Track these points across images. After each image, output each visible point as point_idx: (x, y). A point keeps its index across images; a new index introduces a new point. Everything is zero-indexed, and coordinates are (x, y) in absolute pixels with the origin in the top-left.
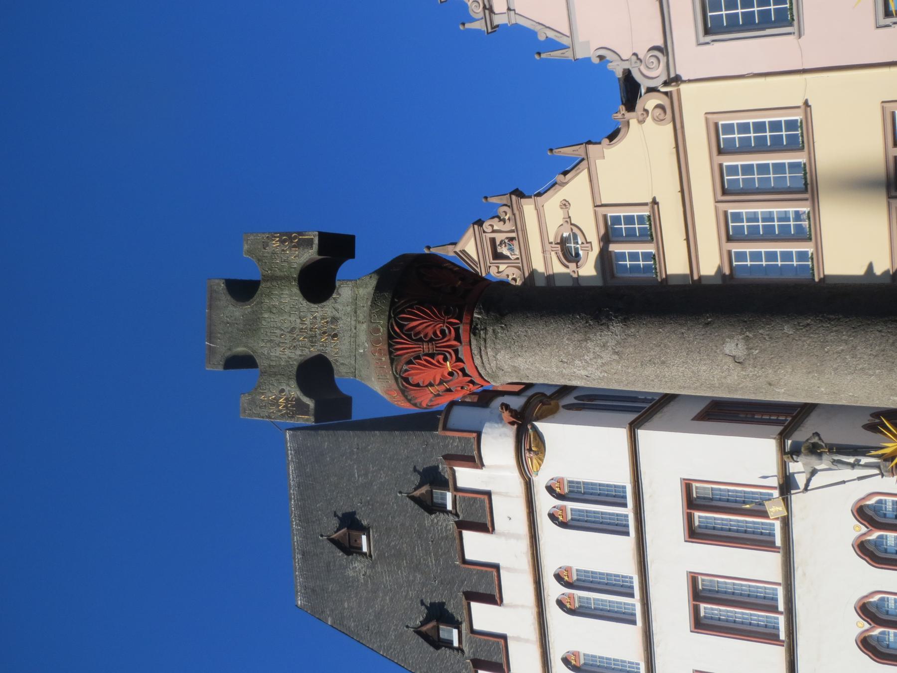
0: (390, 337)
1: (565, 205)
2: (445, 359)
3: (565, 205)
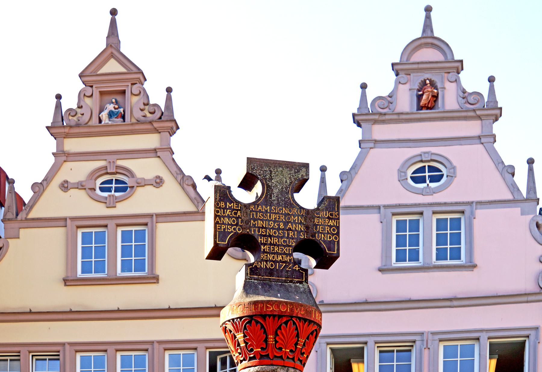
0: (280, 316)
1: (158, 182)
2: (262, 348)
3: (158, 182)
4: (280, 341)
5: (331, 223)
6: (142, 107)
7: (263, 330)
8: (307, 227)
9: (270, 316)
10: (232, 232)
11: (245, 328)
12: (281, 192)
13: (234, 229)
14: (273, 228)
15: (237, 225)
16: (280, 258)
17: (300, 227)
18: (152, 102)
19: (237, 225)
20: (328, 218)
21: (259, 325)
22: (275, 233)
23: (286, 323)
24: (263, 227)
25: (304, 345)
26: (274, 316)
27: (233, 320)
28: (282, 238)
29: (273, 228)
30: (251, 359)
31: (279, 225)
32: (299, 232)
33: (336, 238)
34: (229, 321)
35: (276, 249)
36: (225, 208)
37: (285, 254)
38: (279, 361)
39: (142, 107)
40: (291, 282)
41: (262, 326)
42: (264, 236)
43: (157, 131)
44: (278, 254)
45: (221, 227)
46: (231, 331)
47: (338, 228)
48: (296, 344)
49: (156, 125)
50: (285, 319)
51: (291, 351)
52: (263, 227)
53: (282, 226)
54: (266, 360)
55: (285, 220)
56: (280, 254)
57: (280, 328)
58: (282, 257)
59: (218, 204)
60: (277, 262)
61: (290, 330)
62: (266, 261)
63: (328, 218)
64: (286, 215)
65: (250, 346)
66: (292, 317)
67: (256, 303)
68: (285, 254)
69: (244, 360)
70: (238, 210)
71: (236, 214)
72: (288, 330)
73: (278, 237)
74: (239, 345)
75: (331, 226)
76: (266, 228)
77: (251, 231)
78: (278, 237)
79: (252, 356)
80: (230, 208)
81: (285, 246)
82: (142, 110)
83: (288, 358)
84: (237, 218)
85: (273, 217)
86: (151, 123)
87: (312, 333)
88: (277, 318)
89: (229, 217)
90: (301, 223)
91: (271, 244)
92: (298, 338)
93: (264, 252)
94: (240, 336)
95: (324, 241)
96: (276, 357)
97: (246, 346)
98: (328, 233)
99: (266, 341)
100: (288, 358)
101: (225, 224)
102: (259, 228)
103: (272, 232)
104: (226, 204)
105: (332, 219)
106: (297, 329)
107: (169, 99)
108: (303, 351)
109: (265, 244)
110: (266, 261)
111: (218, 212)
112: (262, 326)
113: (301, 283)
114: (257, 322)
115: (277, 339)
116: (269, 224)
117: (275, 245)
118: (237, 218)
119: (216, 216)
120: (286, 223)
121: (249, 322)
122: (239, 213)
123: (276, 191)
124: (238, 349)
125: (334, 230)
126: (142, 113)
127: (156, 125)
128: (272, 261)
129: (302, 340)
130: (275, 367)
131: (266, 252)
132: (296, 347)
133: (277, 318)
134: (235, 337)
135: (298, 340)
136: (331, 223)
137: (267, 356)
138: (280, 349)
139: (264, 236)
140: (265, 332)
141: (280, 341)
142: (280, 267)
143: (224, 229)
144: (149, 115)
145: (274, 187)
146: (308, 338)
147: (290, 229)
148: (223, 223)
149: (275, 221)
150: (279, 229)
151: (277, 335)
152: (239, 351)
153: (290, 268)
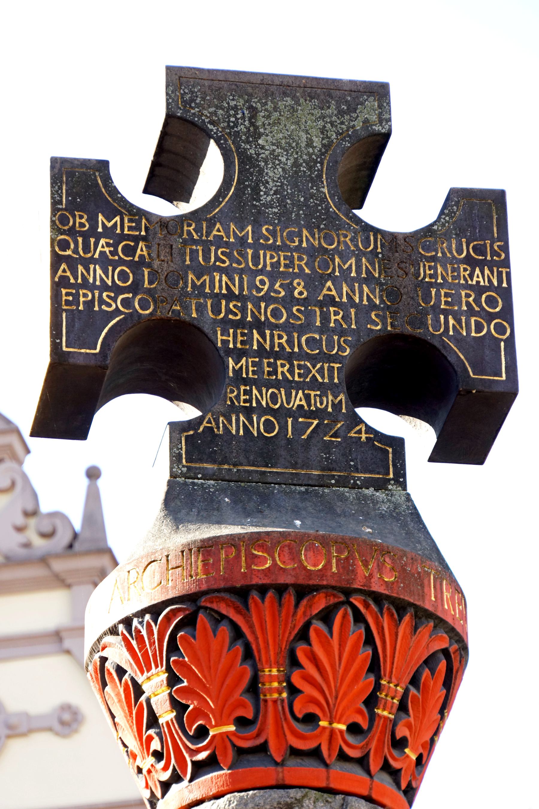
0: (303, 591)
1: (67, 721)
2: (241, 722)
3: (67, 721)
4: (308, 689)
5: (479, 278)
6: (20, 520)
7: (239, 647)
8: (393, 294)
9: (263, 590)
10: (117, 312)
11: (173, 648)
12: (294, 176)
13: (126, 303)
14: (267, 299)
15: (135, 288)
16: (298, 399)
17: (365, 294)
18: (45, 508)
19: (135, 288)
20: (468, 260)
21: (224, 628)
22: (276, 314)
23: (327, 617)
24: (230, 296)
25: (403, 707)
26: (281, 589)
27: (127, 622)
28: (302, 330)
29: (267, 299)
30: (200, 768)
31: (290, 288)
32: (364, 311)
33: (500, 329)
34: (113, 631)
35: (283, 369)
36: (93, 232)
37: (314, 384)
38: (309, 771)
39: (20, 520)
40: (342, 482)
41: (238, 633)
42: (236, 325)
43: (61, 582)
44: (289, 386)
45: (76, 296)
46: (121, 671)
47: (507, 294)
48: (371, 701)
49: (58, 566)
50: (321, 603)
51: (354, 729)
52: (230, 296)
53: (300, 290)
54: (261, 770)
55: (312, 269)
56: (299, 386)
57: (303, 635)
58: (307, 397)
59: (64, 220)
60: (289, 413)
61: (342, 645)
62: (248, 412)
63: (468, 260)
64: (313, 253)
65: (198, 713)
66: (348, 592)
67: (207, 548)
68: (314, 384)
69: (176, 778)
70: (137, 239)
71: (130, 251)
72: (337, 649)
73: (287, 328)
74: (153, 721)
75: (479, 290)
76: (240, 297)
77: (186, 308)
78: (287, 328)
79: (202, 756)
80: (108, 232)
81: (314, 359)
82: (20, 529)
83: (343, 757)
84: (137, 267)
85: (267, 259)
86: (44, 560)
87: (430, 662)
88: (290, 597)
89: (104, 262)
90: (369, 280)
91: (262, 352)
92: (379, 678)
93: (239, 379)
94: (155, 686)
95: (458, 339)
96: (295, 752)
97: (179, 718)
98: (471, 312)
99: (254, 688)
100: (343, 757)
101: (92, 288)
102: (217, 297)
103: (266, 312)
104: (93, 221)
105: (481, 264)
106: (369, 640)
107: (93, 498)
108: (402, 732)
109: (239, 354)
110: (248, 412)
111: (64, 245)
112: (238, 633)
113: (381, 485)
114: (219, 618)
115: (296, 680)
116: (252, 286)
117: (277, 356)
118: (137, 267)
119: (56, 261)
120: (314, 282)
121: (189, 622)
122: (142, 250)
123: (273, 174)
124: (150, 739)
125: (491, 302)
126: (20, 538)
127: (58, 566)
128: (269, 410)
129: (393, 689)
130: (292, 792)
131: (246, 381)
132: (373, 717)
133: (290, 597)
134: (139, 691)
135: (378, 687)
136: (479, 278)
137: (263, 748)
138: (310, 719)
139: (236, 325)
140: (248, 654)
141: (308, 689)
142: (299, 429)
143: (90, 304)
144: (38, 542)
145: (266, 161)
146: (415, 681)
147: (331, 301)
148: (85, 284)
149: (274, 276)
150: (290, 300)
151: (294, 663)
152: (156, 745)
153: (335, 435)
